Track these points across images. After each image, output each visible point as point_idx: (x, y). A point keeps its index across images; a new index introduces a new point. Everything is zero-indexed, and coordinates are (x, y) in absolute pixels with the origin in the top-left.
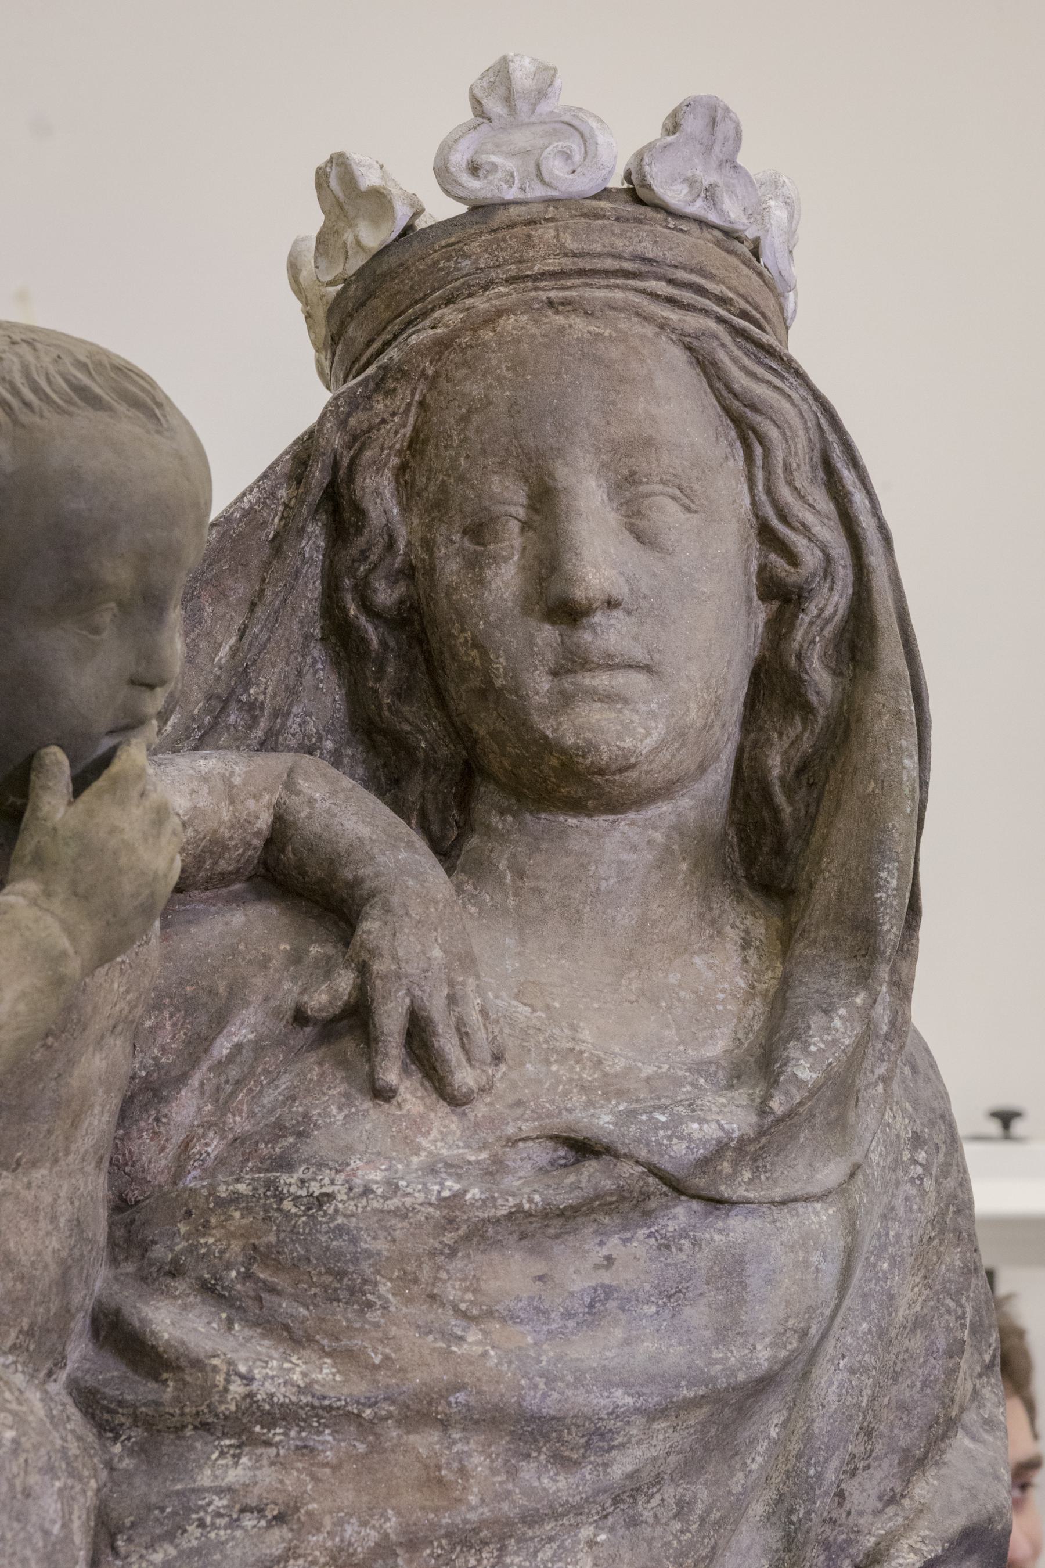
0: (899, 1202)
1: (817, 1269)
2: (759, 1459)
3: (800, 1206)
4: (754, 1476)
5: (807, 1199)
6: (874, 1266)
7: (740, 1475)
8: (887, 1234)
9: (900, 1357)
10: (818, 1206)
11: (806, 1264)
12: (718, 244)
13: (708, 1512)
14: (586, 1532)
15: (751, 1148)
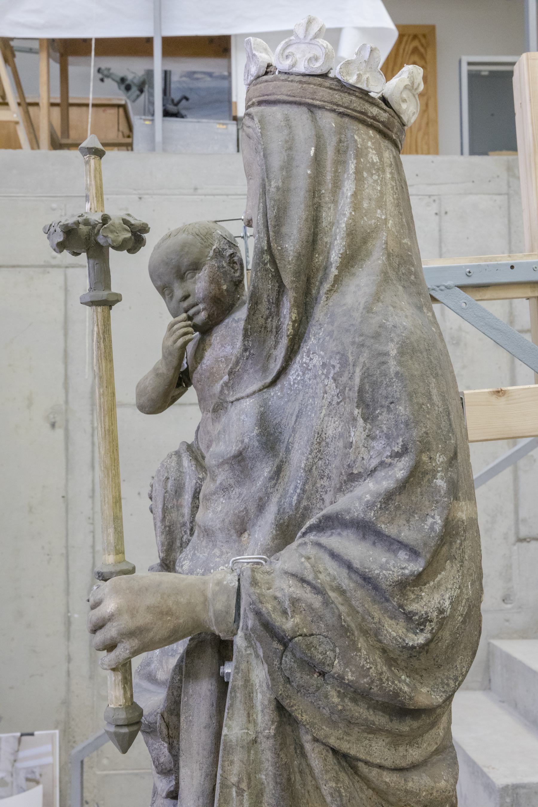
0: (318, 391)
1: (243, 420)
2: (260, 483)
3: (242, 401)
4: (257, 488)
5: (242, 398)
6: (310, 415)
7: (254, 487)
8: (315, 403)
9: (336, 449)
10: (248, 399)
11: (239, 419)
12: (254, 85)
13: (244, 498)
14: (222, 499)
15: (230, 385)
